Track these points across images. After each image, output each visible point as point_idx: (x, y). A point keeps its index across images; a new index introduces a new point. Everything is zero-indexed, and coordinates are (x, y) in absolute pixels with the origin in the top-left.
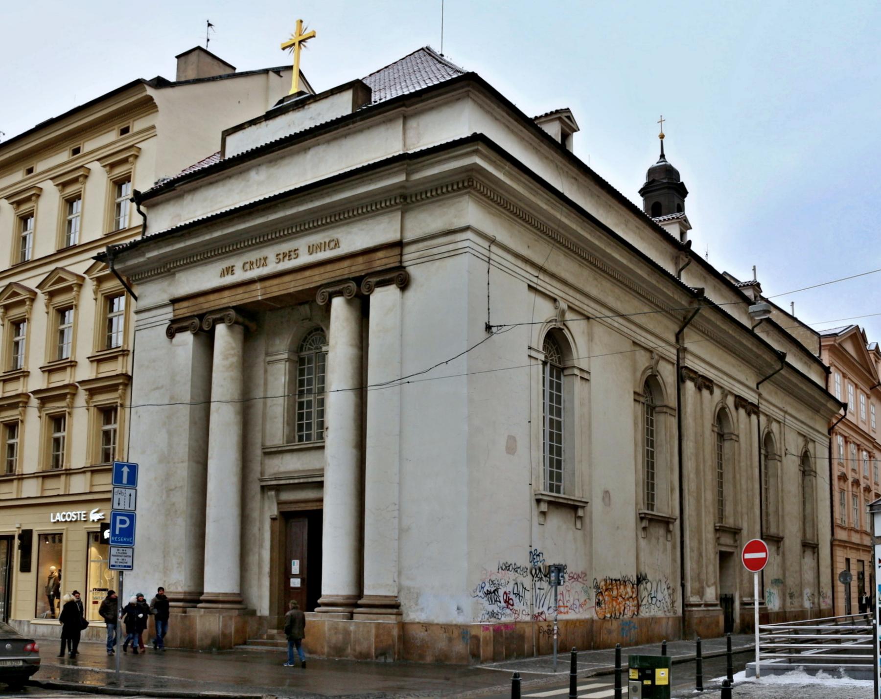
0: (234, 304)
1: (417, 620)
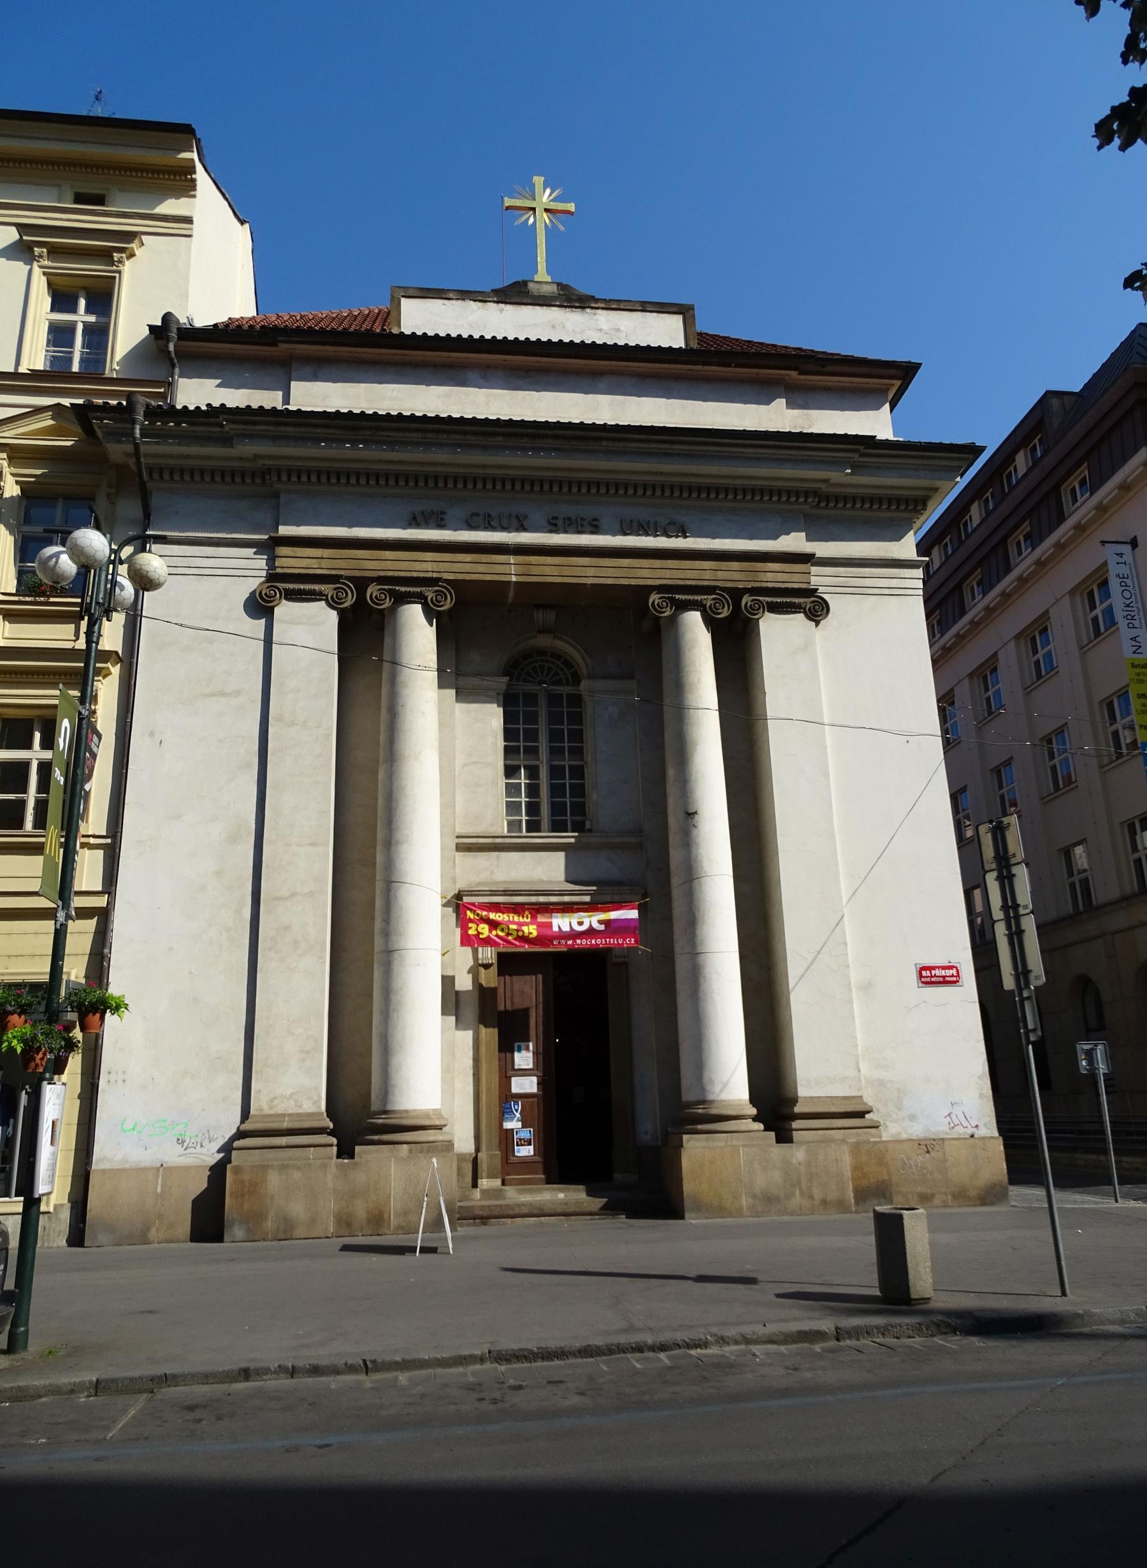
0: (451, 577)
1: (904, 1136)
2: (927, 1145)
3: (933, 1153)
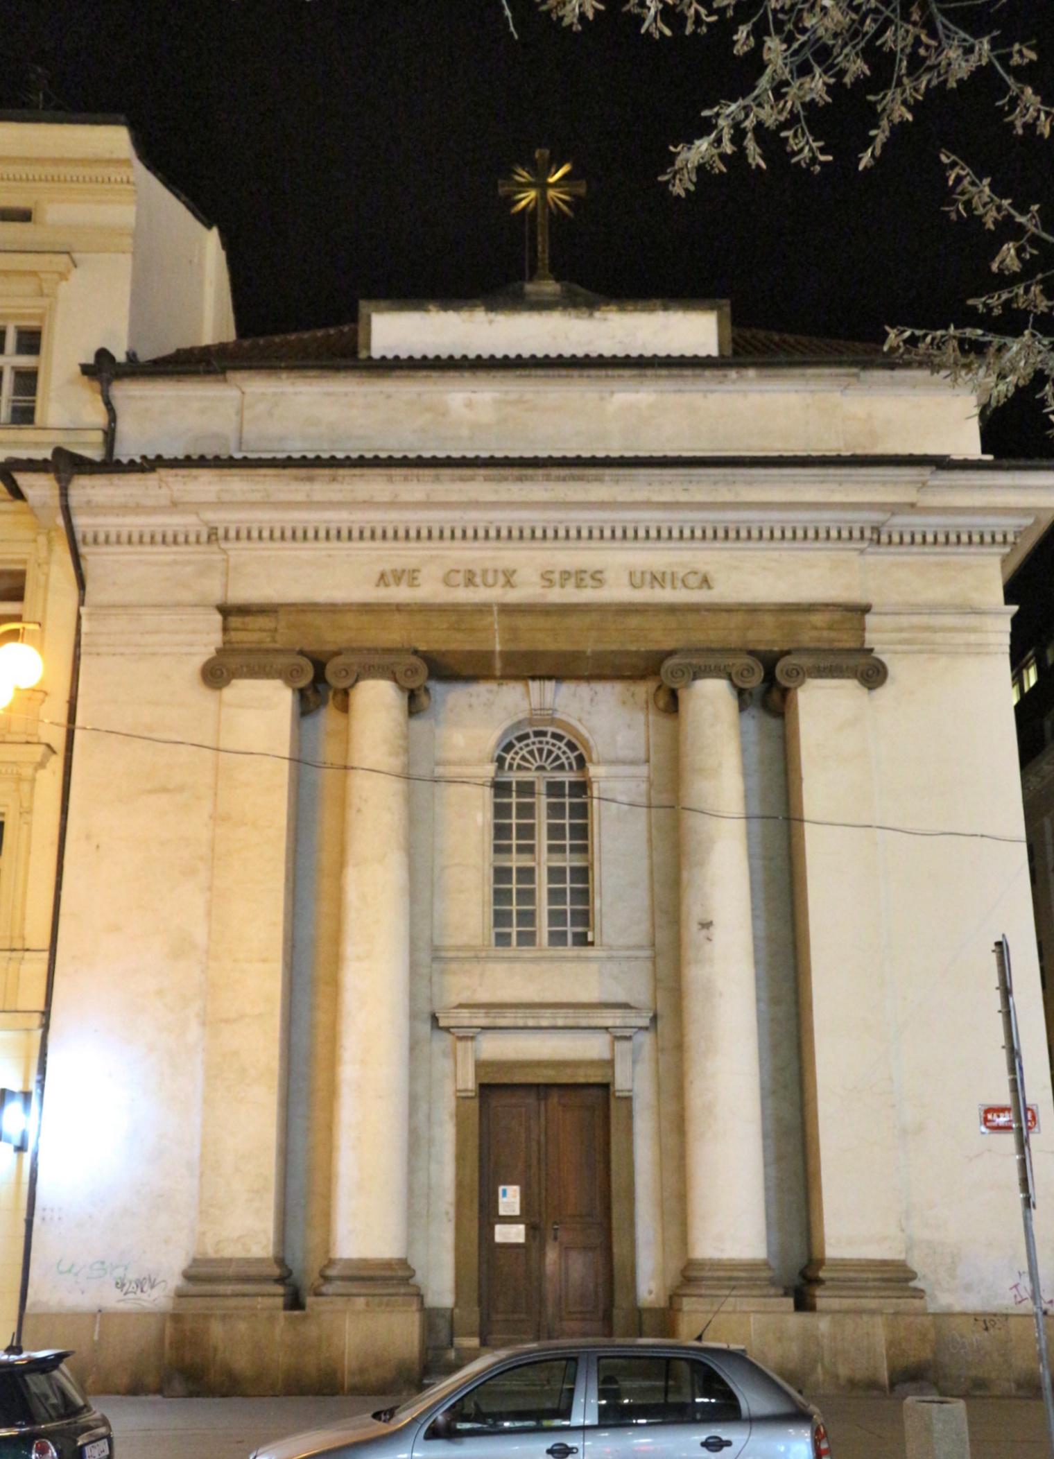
2: (987, 1320)
3: (991, 1331)
